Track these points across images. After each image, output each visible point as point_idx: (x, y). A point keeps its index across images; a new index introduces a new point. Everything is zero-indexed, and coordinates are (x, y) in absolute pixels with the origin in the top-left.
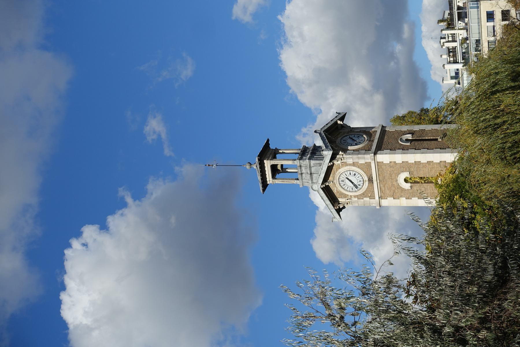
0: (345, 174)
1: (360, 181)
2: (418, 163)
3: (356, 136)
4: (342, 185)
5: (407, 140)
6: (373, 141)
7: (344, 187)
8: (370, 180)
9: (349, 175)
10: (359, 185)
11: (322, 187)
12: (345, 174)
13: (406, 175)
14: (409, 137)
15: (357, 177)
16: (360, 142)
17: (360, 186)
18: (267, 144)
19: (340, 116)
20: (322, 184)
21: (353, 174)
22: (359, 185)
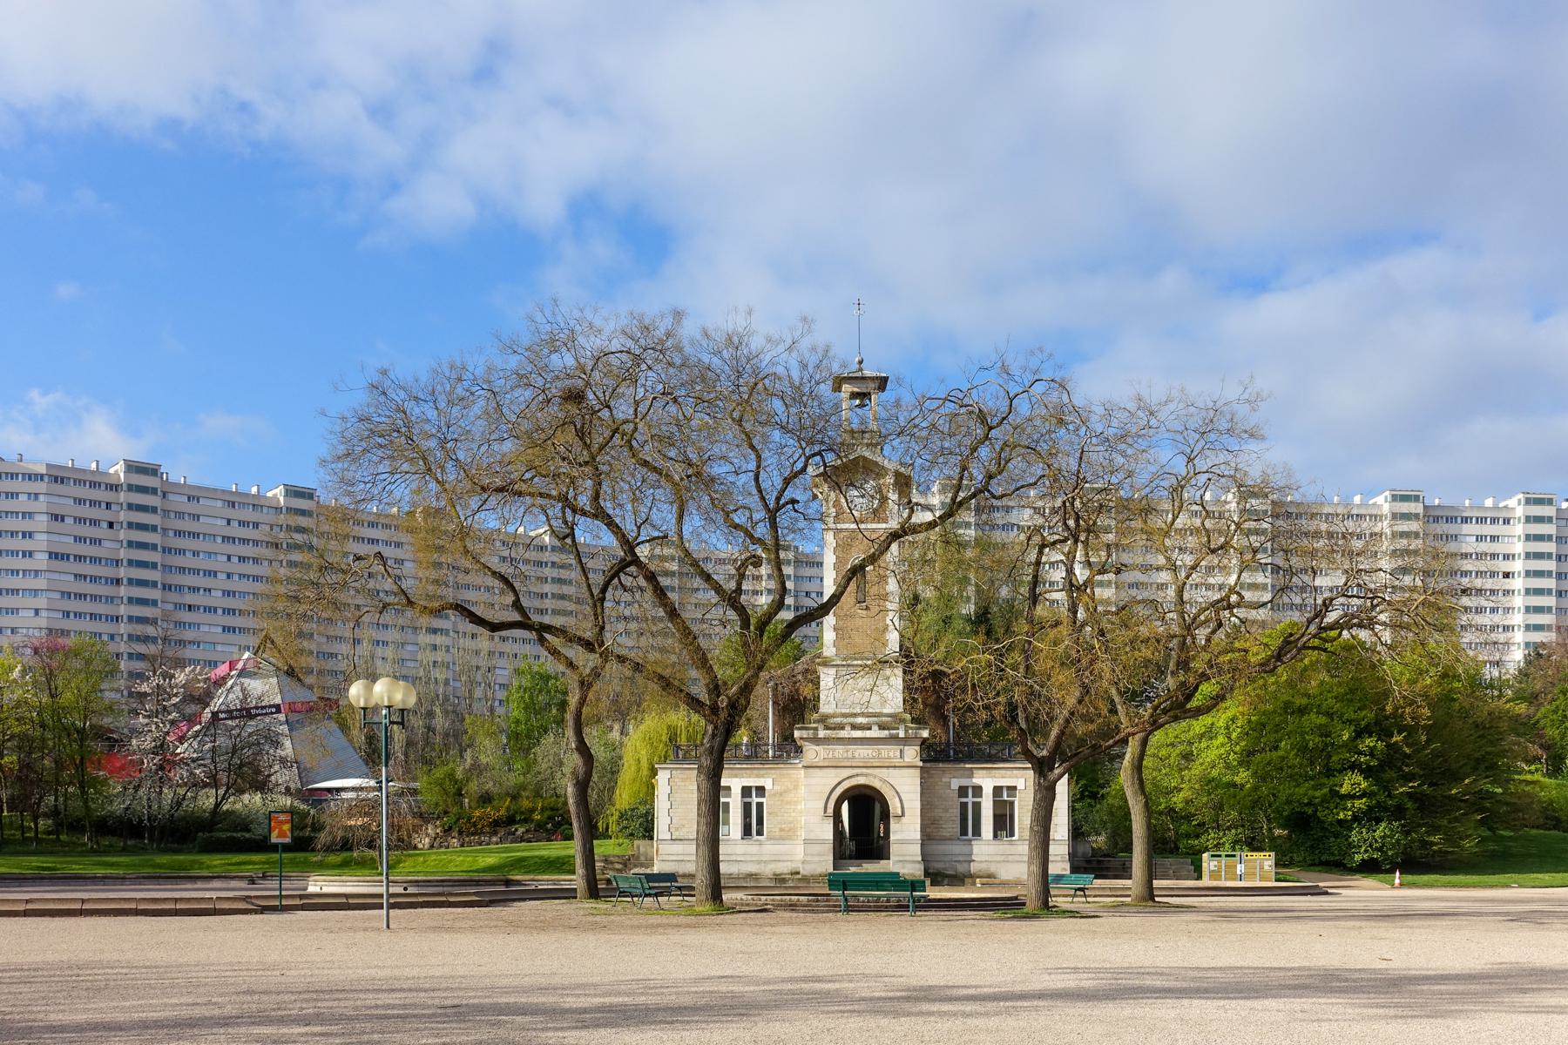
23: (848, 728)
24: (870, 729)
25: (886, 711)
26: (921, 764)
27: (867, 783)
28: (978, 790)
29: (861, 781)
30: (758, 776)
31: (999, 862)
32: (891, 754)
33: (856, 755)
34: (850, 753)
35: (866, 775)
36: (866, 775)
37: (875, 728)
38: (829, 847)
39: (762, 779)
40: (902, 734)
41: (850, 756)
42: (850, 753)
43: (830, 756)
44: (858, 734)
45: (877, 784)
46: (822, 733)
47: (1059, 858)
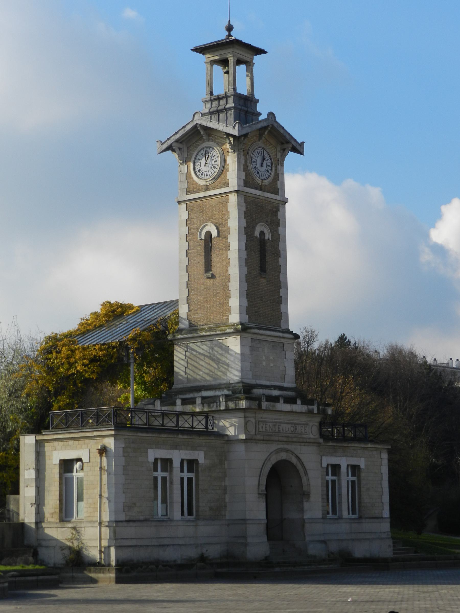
0: (215, 155)
1: (207, 175)
2: (228, 247)
3: (270, 168)
4: (202, 152)
5: (262, 233)
6: (261, 190)
7: (200, 154)
8: (207, 188)
9: (214, 161)
10: (202, 174)
11: (198, 126)
12: (215, 155)
13: (214, 234)
14: (268, 236)
15: (211, 170)
16: (258, 173)
17: (202, 175)
18: (260, 51)
19: (298, 147)
20: (201, 126)
21: (215, 166)
22: (202, 174)
23: (282, 401)
24: (295, 403)
25: (285, 385)
26: (321, 440)
27: (288, 459)
28: (336, 468)
29: (284, 456)
30: (194, 448)
31: (353, 540)
32: (303, 430)
33: (281, 429)
34: (277, 427)
35: (287, 451)
36: (287, 451)
37: (299, 402)
38: (262, 528)
39: (196, 452)
40: (315, 411)
41: (277, 430)
42: (277, 427)
43: (264, 430)
44: (287, 407)
45: (294, 460)
46: (264, 404)
47: (384, 536)
